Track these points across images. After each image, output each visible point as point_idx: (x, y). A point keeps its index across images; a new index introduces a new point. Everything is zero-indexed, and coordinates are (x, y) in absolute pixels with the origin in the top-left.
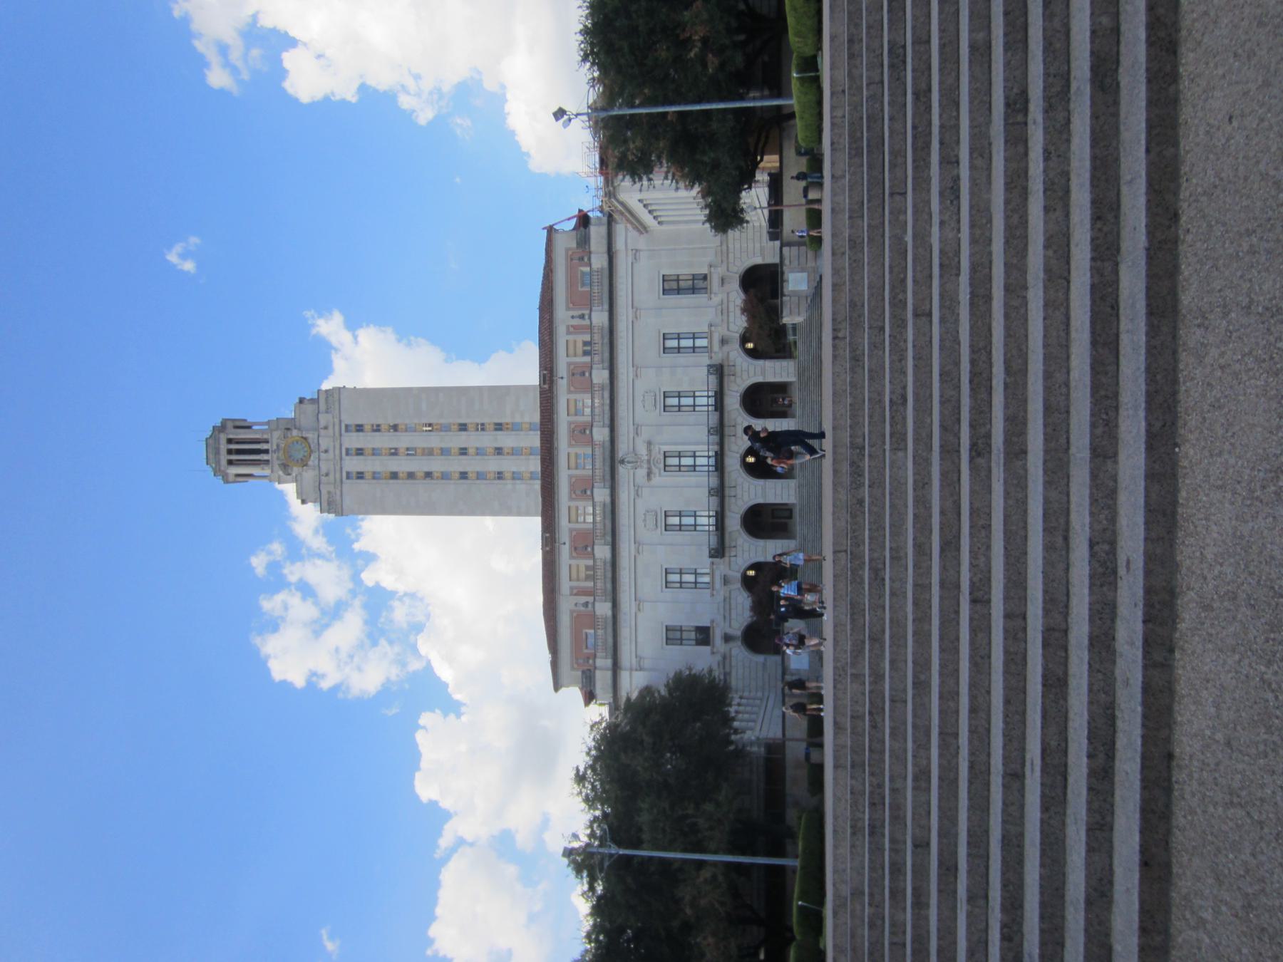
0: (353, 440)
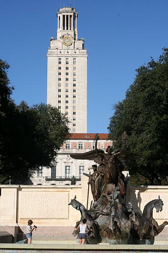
0: (70, 60)
